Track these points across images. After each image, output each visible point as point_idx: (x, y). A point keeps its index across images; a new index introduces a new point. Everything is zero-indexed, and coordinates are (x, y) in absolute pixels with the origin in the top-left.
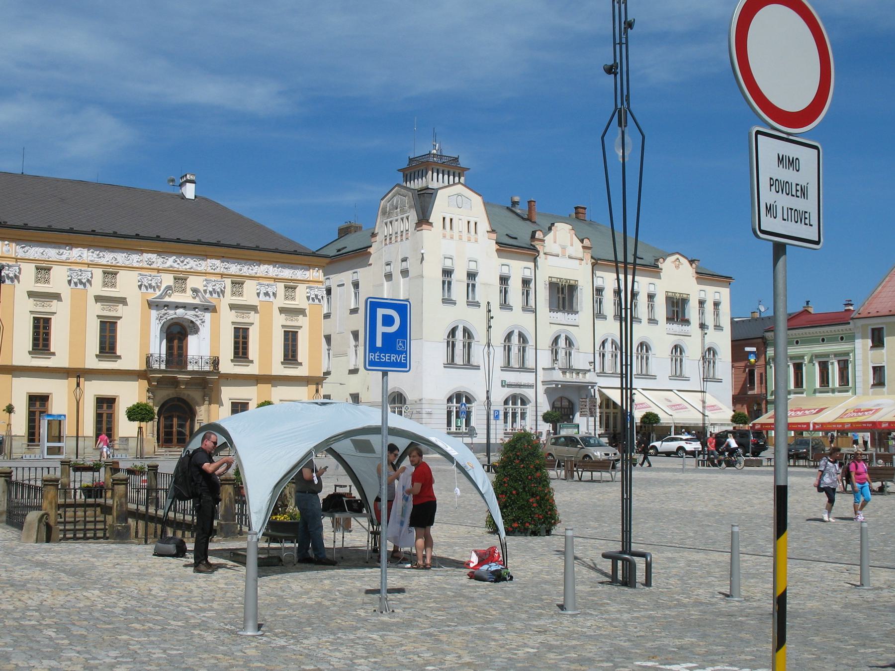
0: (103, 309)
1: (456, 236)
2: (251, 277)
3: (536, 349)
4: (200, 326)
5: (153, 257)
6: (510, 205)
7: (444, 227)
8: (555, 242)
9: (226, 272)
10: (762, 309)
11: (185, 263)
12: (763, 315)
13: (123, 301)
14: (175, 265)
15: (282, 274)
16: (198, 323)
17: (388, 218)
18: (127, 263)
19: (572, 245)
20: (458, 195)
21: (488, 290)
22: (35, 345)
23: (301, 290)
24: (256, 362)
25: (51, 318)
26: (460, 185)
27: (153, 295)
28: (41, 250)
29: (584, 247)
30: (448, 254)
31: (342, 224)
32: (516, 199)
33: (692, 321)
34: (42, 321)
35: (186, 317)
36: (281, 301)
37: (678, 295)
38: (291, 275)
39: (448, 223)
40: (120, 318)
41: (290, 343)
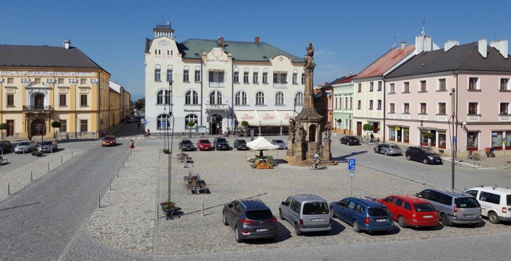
2: (66, 77)
21: (178, 77)
23: (88, 80)
29: (228, 56)
37: (281, 72)
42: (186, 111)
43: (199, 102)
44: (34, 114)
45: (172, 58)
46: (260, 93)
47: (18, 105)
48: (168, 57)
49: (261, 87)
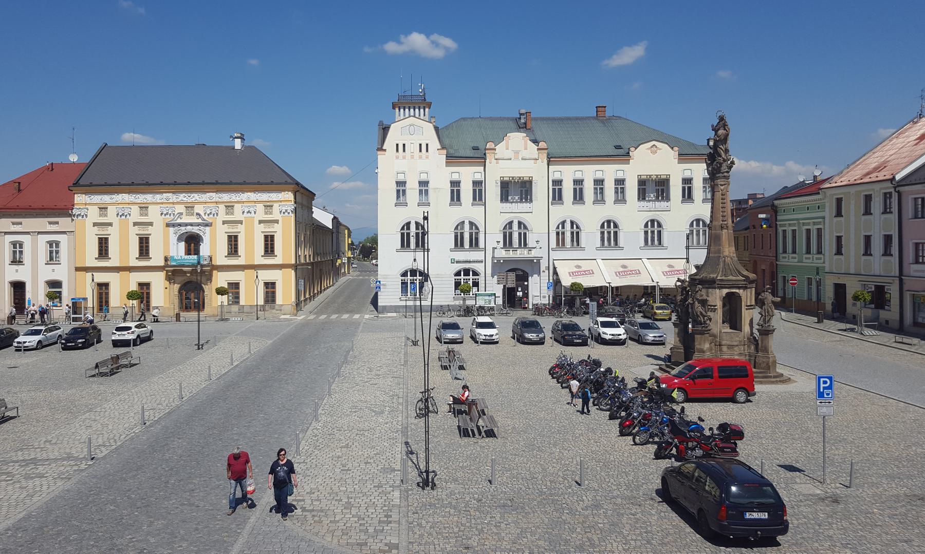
0: (99, 230)
3: (485, 234)
4: (203, 236)
5: (170, 195)
7: (420, 151)
8: (507, 149)
9: (220, 200)
11: (192, 197)
13: (151, 224)
14: (185, 199)
15: (261, 198)
16: (201, 234)
18: (154, 201)
19: (526, 149)
22: (266, 251)
25: (238, 235)
26: (412, 117)
27: (169, 219)
28: (99, 197)
30: (401, 170)
34: (233, 237)
35: (193, 231)
38: (267, 198)
41: (269, 243)
42: (453, 261)
43: (481, 245)
44: (185, 272)
45: (427, 157)
46: (609, 222)
47: (156, 258)
48: (420, 157)
49: (610, 210)
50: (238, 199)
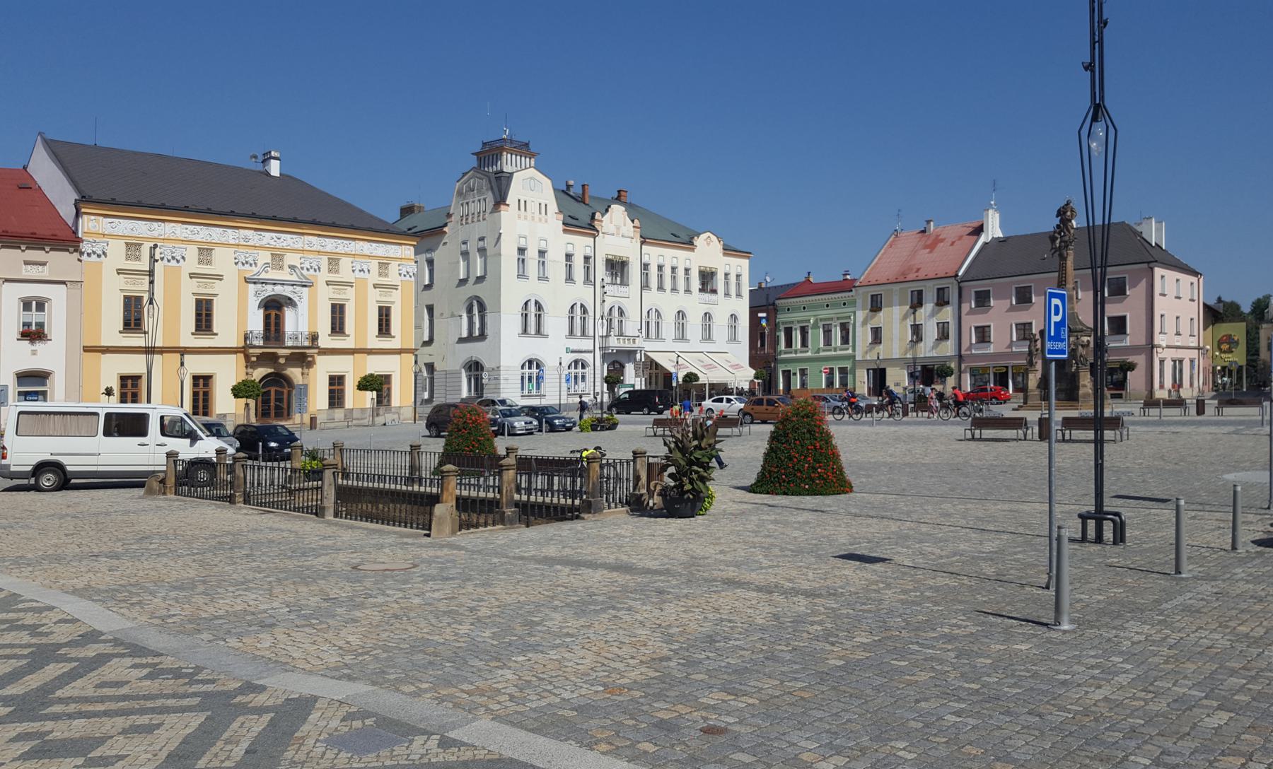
1: (529, 218)
2: (346, 254)
4: (298, 303)
6: (565, 189)
9: (322, 249)
10: (768, 280)
11: (282, 240)
12: (768, 285)
13: (219, 278)
14: (272, 242)
17: (464, 199)
18: (223, 240)
19: (625, 225)
20: (531, 178)
23: (394, 267)
24: (352, 336)
26: (532, 169)
29: (634, 227)
30: (523, 233)
31: (404, 204)
32: (571, 182)
33: (719, 292)
35: (284, 294)
36: (374, 278)
37: (708, 269)
39: (522, 205)
40: (216, 295)
50: (348, 250)
